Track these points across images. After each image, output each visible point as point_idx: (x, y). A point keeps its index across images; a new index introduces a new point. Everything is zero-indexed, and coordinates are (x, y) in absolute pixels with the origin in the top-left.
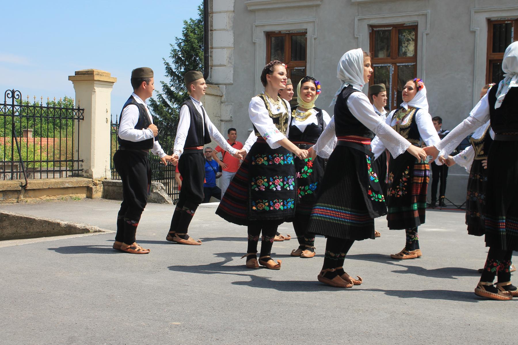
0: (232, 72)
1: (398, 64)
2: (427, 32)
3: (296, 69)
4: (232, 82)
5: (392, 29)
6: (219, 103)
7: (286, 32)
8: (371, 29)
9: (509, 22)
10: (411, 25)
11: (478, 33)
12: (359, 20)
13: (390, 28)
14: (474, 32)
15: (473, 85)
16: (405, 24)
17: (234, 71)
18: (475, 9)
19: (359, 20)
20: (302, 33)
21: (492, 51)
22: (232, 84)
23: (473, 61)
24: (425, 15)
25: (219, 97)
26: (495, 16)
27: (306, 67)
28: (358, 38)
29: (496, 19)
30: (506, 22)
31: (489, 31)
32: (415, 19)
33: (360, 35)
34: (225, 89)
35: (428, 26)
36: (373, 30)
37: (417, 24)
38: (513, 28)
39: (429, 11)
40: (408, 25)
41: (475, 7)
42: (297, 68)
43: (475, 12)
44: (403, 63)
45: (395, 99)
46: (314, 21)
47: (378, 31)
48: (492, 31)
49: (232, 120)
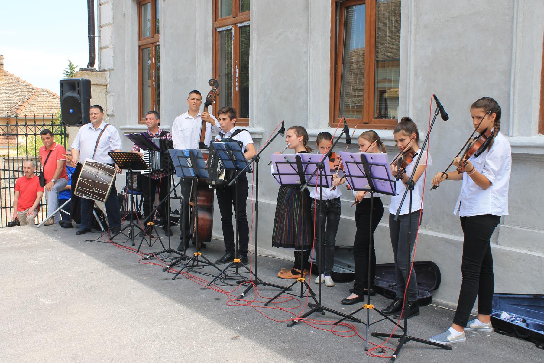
0: (112, 55)
1: (239, 25)
4: (112, 67)
6: (103, 94)
17: (114, 54)
22: (113, 70)
25: (102, 86)
34: (109, 77)
44: (242, 22)
45: (237, 80)
49: (114, 114)
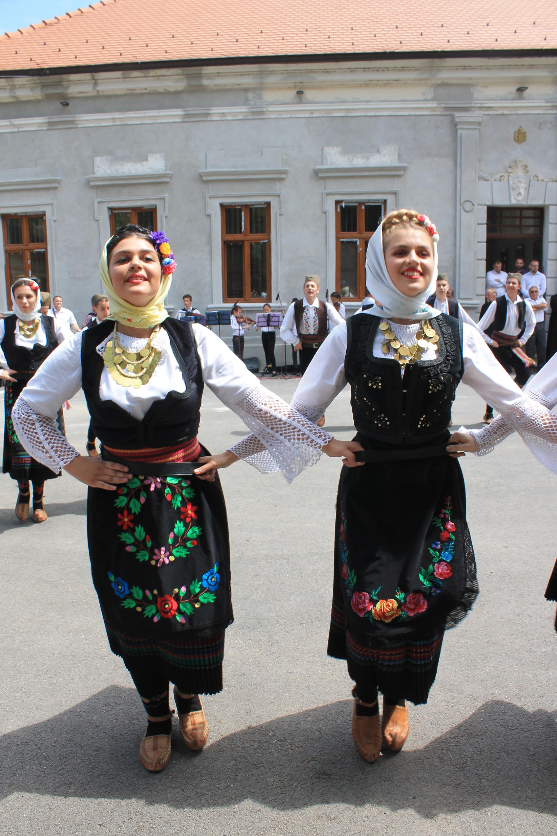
2: (166, 215)
3: (36, 252)
5: (131, 212)
7: (23, 214)
8: (110, 211)
9: (239, 207)
10: (149, 208)
11: (213, 216)
12: (99, 203)
13: (129, 211)
14: (209, 216)
15: (211, 264)
16: (143, 207)
18: (209, 194)
19: (99, 203)
20: (40, 215)
21: (225, 233)
23: (210, 242)
24: (163, 199)
26: (227, 201)
27: (46, 249)
28: (98, 220)
29: (228, 204)
30: (237, 207)
31: (222, 215)
32: (153, 202)
33: (100, 218)
35: (167, 209)
36: (112, 212)
37: (155, 207)
38: (243, 214)
39: (166, 195)
40: (146, 208)
41: (209, 193)
42: (37, 250)
43: (210, 198)
46: (52, 204)
47: (119, 214)
48: (225, 214)
